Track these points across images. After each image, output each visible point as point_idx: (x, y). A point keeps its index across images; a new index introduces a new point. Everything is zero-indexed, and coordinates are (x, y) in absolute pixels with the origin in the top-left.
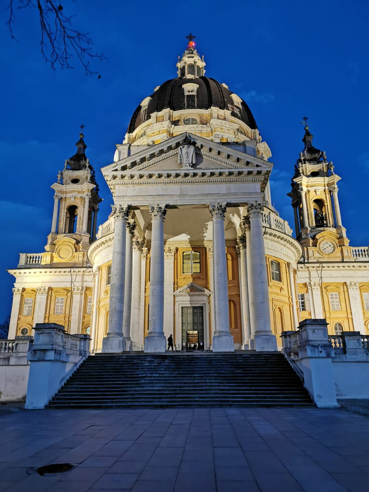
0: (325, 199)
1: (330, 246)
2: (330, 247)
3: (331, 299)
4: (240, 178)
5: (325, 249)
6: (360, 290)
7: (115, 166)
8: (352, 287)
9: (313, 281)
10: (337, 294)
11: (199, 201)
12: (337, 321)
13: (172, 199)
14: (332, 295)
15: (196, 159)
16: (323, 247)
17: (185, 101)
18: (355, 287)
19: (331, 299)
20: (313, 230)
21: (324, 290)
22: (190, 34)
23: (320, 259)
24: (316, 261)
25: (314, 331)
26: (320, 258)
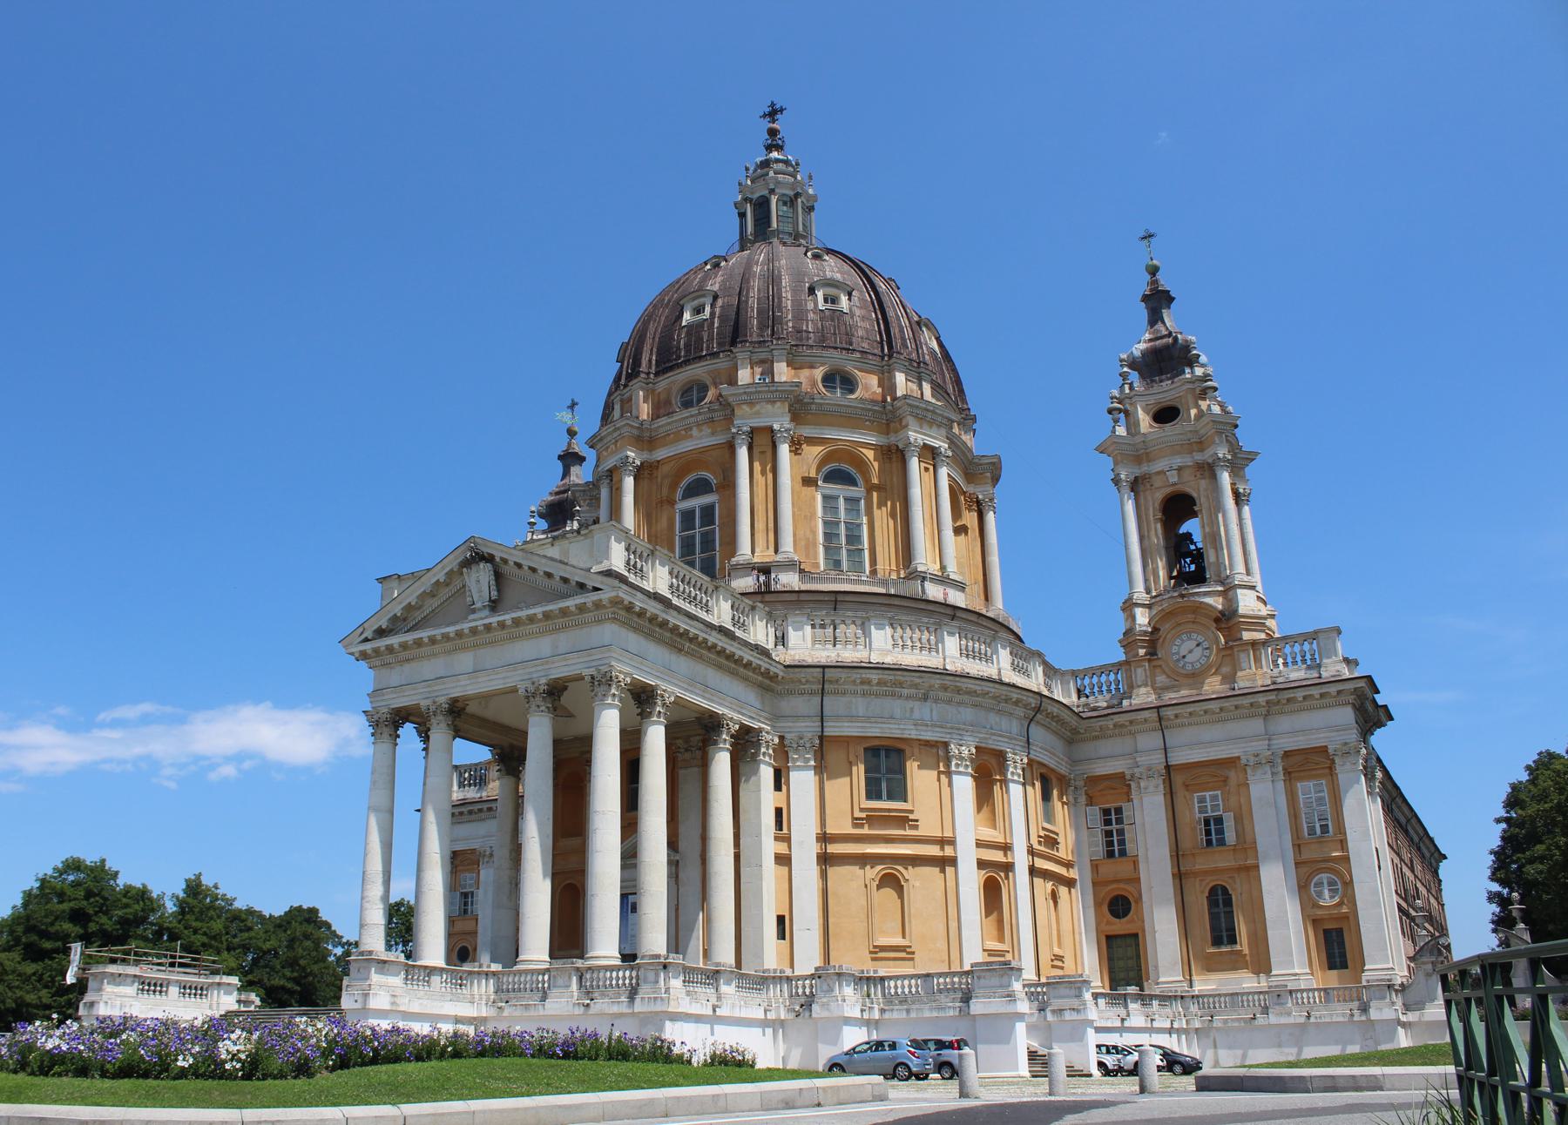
0: (1195, 495)
1: (1198, 645)
2: (1200, 648)
3: (1200, 812)
4: (572, 620)
5: (1184, 657)
6: (1288, 773)
7: (362, 633)
10: (1217, 796)
11: (501, 682)
12: (1212, 881)
13: (458, 684)
14: (1202, 800)
15: (499, 591)
16: (1178, 653)
18: (1267, 768)
20: (1153, 600)
25: (359, 971)
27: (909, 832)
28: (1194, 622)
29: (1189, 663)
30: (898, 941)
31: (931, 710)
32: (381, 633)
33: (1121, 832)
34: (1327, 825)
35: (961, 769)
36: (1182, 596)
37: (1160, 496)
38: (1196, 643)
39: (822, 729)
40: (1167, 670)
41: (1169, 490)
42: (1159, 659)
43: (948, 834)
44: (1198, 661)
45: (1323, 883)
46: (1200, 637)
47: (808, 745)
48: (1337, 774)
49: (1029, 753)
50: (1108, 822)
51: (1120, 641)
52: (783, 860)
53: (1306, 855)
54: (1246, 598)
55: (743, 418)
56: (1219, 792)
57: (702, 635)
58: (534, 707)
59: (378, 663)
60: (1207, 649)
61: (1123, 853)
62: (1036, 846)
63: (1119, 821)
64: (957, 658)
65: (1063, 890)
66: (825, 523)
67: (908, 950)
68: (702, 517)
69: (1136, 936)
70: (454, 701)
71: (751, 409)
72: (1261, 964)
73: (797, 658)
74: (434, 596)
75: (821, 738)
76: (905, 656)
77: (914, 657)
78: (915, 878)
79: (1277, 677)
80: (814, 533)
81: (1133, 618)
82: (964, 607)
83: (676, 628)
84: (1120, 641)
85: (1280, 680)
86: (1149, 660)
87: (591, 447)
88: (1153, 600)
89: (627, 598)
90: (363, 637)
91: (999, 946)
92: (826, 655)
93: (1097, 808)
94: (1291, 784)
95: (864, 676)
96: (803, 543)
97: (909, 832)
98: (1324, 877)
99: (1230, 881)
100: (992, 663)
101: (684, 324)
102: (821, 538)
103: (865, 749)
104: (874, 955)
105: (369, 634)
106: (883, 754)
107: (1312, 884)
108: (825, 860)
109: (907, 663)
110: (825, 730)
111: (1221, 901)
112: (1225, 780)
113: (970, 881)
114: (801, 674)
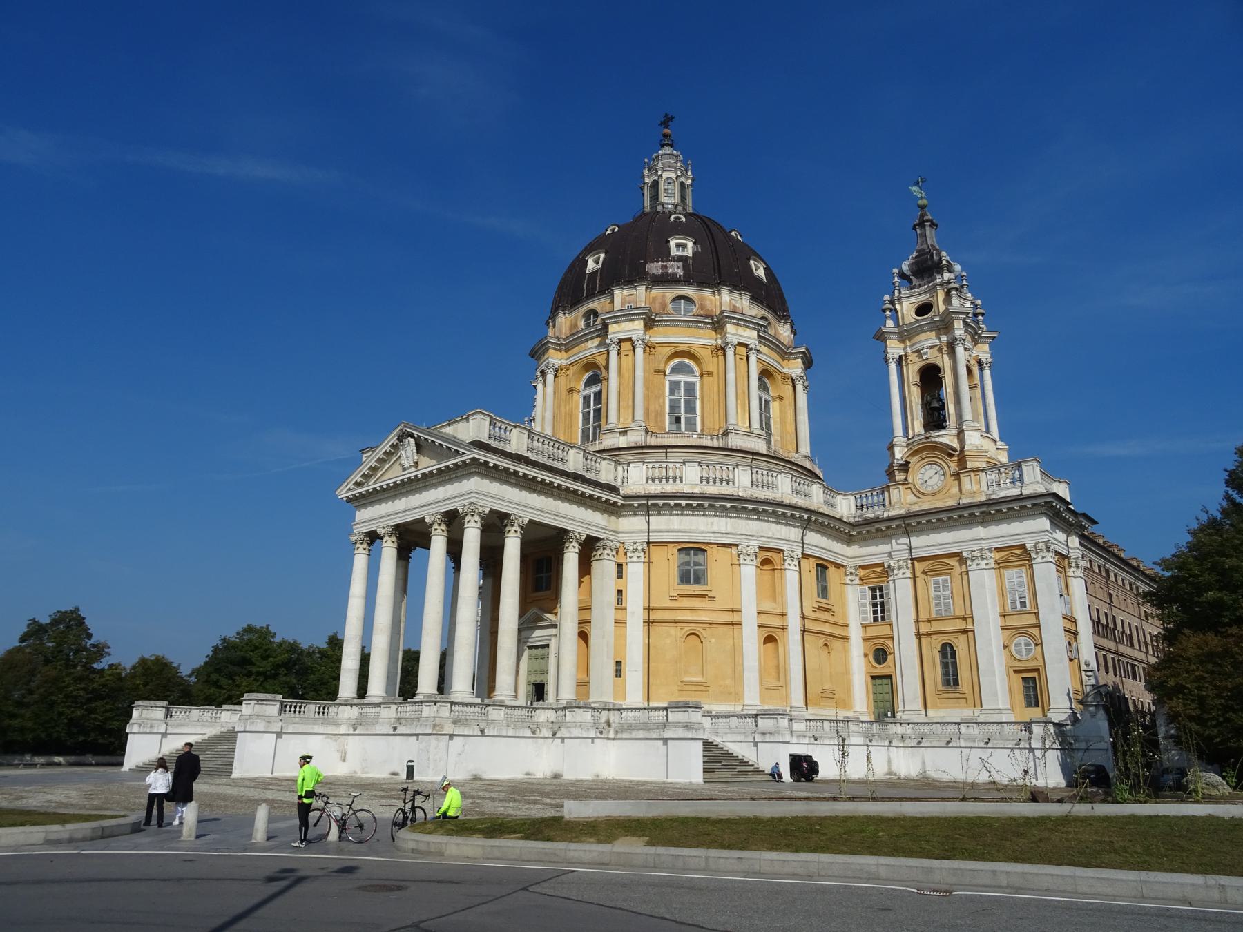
0: (941, 366)
1: (936, 473)
3: (935, 591)
5: (926, 481)
6: (997, 562)
8: (1041, 554)
9: (896, 556)
14: (936, 583)
16: (922, 479)
17: (585, 285)
19: (935, 591)
21: (918, 574)
22: (666, 115)
23: (913, 507)
24: (902, 512)
26: (914, 504)
27: (710, 605)
28: (933, 457)
29: (929, 486)
30: (699, 679)
31: (726, 523)
32: (358, 484)
33: (882, 604)
34: (1025, 602)
35: (748, 562)
36: (926, 438)
37: (917, 367)
38: (935, 471)
39: (649, 536)
40: (914, 491)
41: (922, 363)
42: (909, 483)
43: (736, 607)
44: (936, 484)
45: (1021, 644)
46: (937, 467)
47: (640, 548)
48: (1032, 564)
49: (803, 550)
50: (874, 597)
51: (886, 472)
52: (620, 623)
53: (1009, 624)
54: (971, 438)
55: (614, 333)
56: (949, 577)
57: (548, 480)
58: (433, 531)
59: (357, 504)
60: (942, 475)
61: (883, 619)
62: (808, 612)
63: (882, 596)
64: (748, 488)
65: (836, 644)
66: (671, 401)
67: (705, 684)
68: (595, 400)
69: (890, 677)
70: (397, 527)
71: (619, 326)
72: (977, 701)
73: (635, 491)
74: (386, 461)
75: (648, 543)
76: (709, 487)
77: (715, 488)
78: (712, 638)
79: (991, 494)
80: (663, 407)
81: (893, 454)
82: (765, 452)
83: (525, 475)
84: (886, 472)
85: (993, 497)
86: (903, 484)
87: (532, 357)
88: (909, 442)
89: (482, 459)
90: (348, 487)
91: (775, 683)
92: (654, 489)
93: (867, 587)
94: (1000, 573)
95: (676, 502)
96: (653, 414)
97: (710, 605)
98: (1023, 639)
99: (956, 640)
100: (778, 490)
101: (587, 272)
102: (667, 410)
103: (679, 550)
104: (680, 688)
105: (351, 486)
106: (692, 552)
107: (1014, 645)
108: (649, 623)
109: (710, 492)
110: (650, 538)
111: (949, 654)
112: (951, 567)
113: (751, 638)
114: (635, 503)
